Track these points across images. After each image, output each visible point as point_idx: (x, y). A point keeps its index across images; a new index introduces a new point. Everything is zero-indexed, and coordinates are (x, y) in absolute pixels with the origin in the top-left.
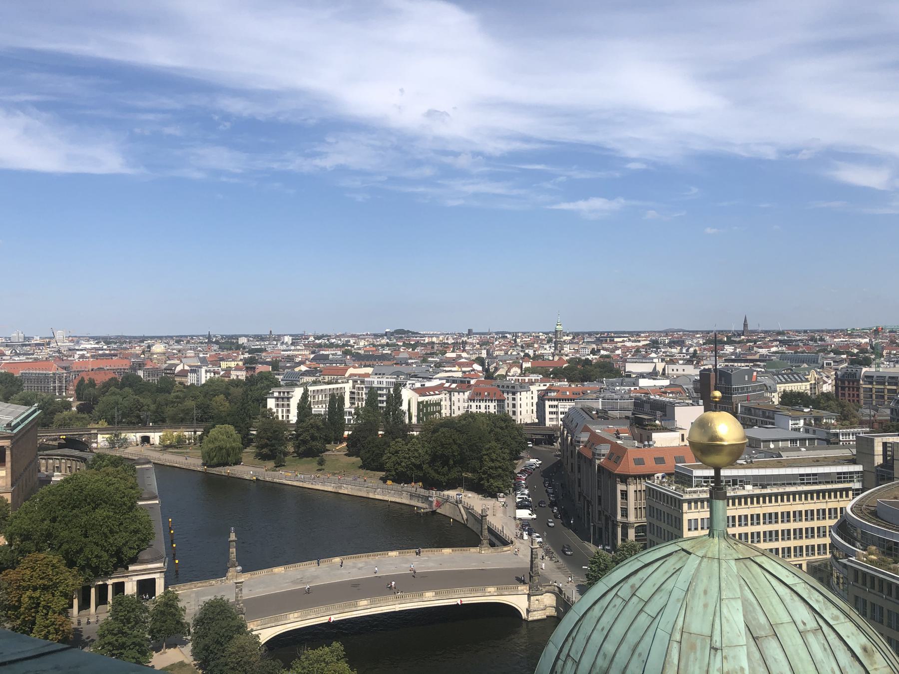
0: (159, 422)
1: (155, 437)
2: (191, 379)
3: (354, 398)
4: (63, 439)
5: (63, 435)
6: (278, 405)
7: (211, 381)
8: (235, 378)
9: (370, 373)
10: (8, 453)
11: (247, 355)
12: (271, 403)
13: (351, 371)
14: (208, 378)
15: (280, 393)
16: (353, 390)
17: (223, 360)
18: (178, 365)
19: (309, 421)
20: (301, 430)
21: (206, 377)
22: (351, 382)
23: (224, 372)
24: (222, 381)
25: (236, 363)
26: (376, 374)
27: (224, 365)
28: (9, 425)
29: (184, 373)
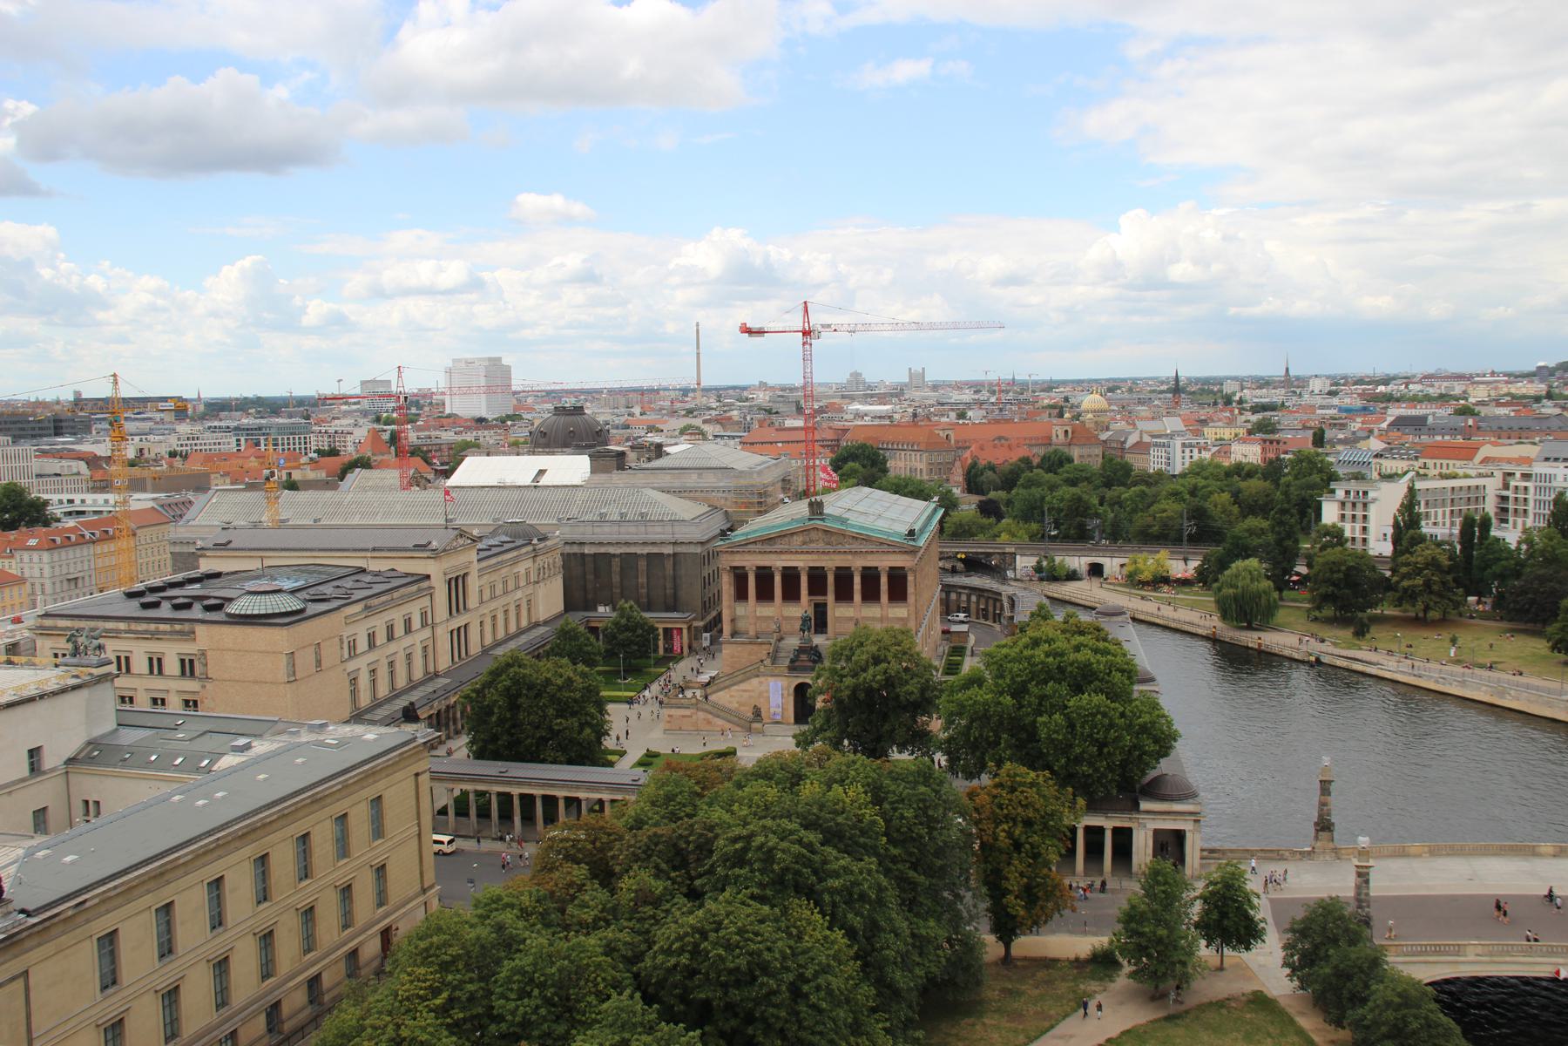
0: (1116, 536)
1: (1111, 564)
2: (1153, 462)
3: (1505, 510)
4: (961, 560)
5: (962, 553)
6: (1343, 516)
7: (1198, 469)
8: (1240, 458)
9: (1533, 456)
10: (910, 578)
11: (1255, 418)
12: (1330, 513)
13: (1486, 451)
14: (1187, 461)
15: (1348, 492)
16: (1505, 493)
17: (1204, 422)
18: (1130, 433)
19: (1421, 555)
20: (1404, 570)
21: (1191, 457)
22: (1499, 475)
23: (1216, 448)
24: (1218, 466)
25: (1233, 431)
26: (1547, 459)
27: (1210, 433)
28: (911, 533)
29: (1142, 447)
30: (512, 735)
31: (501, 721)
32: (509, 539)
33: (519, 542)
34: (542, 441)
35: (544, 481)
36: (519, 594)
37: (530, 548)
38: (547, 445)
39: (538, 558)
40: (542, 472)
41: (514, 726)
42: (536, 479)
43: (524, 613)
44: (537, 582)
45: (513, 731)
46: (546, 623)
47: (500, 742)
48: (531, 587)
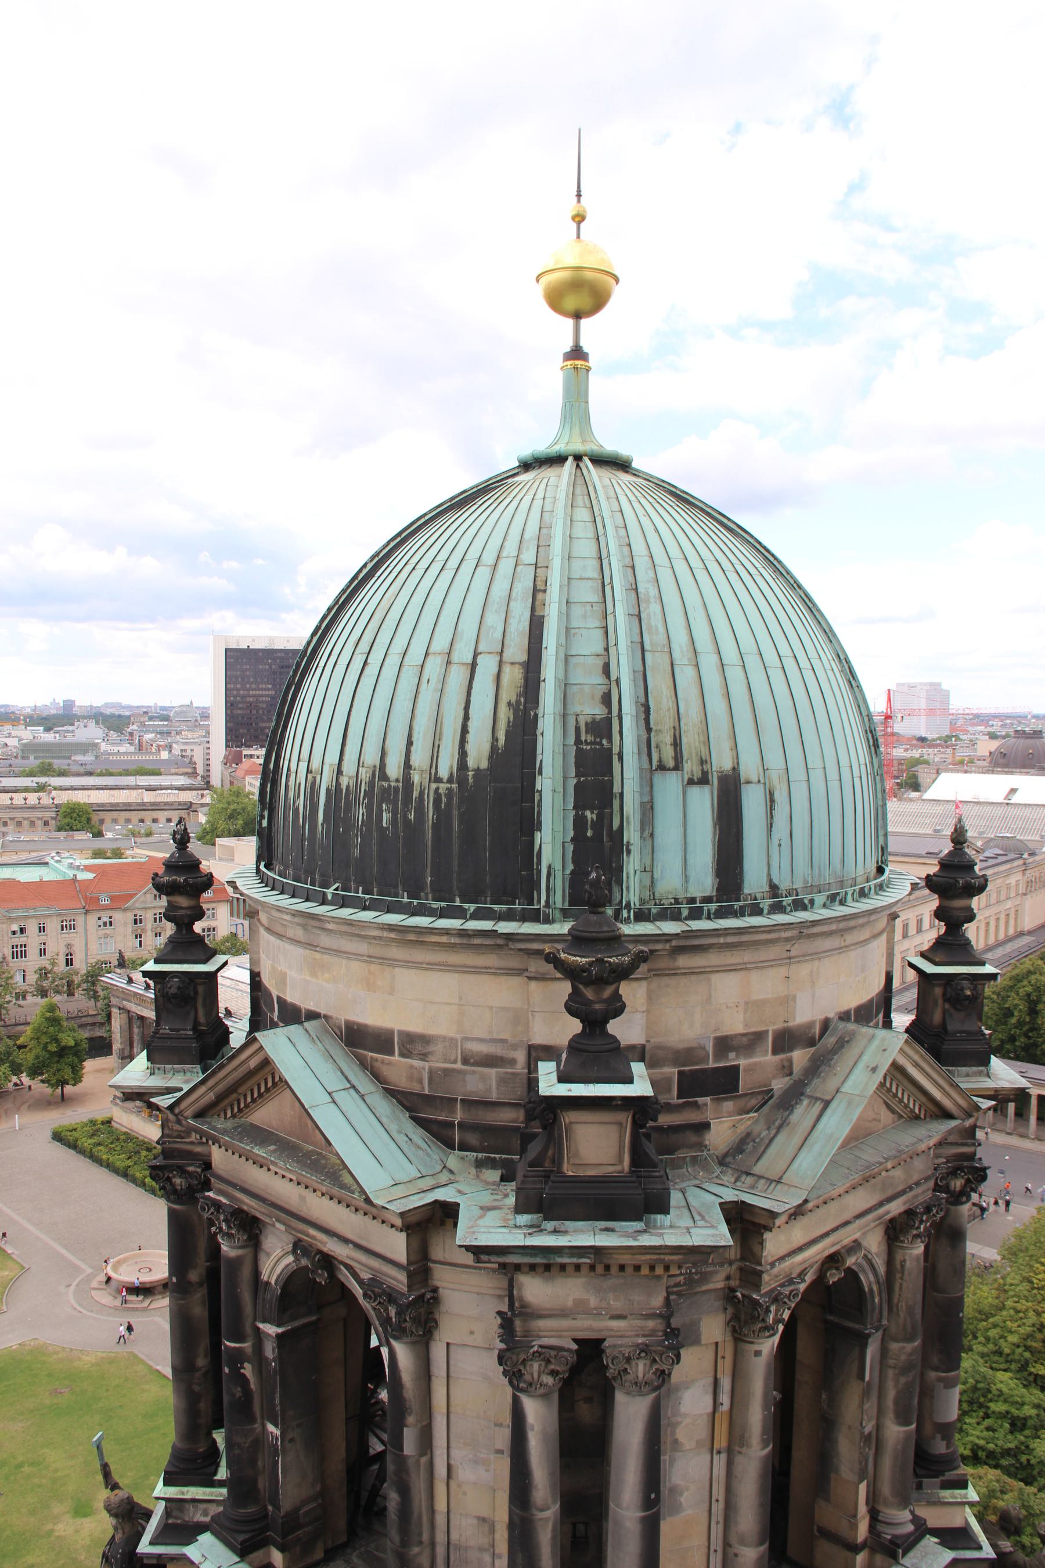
30: (1029, 1038)
31: (1020, 1024)
32: (1001, 852)
33: (1011, 856)
34: (1001, 761)
35: (1016, 799)
36: (1009, 904)
37: (1021, 862)
38: (1006, 766)
39: (1028, 872)
40: (1013, 791)
41: (1032, 1029)
42: (1007, 797)
43: (1012, 922)
44: (1025, 894)
45: (1030, 1034)
46: (1030, 933)
47: (1017, 1043)
48: (1019, 898)
